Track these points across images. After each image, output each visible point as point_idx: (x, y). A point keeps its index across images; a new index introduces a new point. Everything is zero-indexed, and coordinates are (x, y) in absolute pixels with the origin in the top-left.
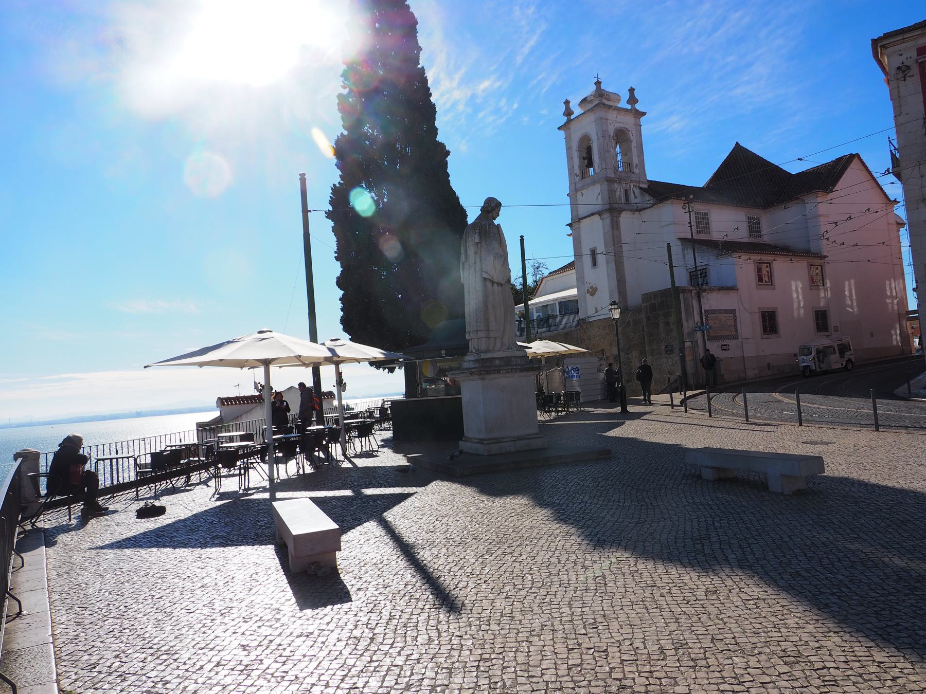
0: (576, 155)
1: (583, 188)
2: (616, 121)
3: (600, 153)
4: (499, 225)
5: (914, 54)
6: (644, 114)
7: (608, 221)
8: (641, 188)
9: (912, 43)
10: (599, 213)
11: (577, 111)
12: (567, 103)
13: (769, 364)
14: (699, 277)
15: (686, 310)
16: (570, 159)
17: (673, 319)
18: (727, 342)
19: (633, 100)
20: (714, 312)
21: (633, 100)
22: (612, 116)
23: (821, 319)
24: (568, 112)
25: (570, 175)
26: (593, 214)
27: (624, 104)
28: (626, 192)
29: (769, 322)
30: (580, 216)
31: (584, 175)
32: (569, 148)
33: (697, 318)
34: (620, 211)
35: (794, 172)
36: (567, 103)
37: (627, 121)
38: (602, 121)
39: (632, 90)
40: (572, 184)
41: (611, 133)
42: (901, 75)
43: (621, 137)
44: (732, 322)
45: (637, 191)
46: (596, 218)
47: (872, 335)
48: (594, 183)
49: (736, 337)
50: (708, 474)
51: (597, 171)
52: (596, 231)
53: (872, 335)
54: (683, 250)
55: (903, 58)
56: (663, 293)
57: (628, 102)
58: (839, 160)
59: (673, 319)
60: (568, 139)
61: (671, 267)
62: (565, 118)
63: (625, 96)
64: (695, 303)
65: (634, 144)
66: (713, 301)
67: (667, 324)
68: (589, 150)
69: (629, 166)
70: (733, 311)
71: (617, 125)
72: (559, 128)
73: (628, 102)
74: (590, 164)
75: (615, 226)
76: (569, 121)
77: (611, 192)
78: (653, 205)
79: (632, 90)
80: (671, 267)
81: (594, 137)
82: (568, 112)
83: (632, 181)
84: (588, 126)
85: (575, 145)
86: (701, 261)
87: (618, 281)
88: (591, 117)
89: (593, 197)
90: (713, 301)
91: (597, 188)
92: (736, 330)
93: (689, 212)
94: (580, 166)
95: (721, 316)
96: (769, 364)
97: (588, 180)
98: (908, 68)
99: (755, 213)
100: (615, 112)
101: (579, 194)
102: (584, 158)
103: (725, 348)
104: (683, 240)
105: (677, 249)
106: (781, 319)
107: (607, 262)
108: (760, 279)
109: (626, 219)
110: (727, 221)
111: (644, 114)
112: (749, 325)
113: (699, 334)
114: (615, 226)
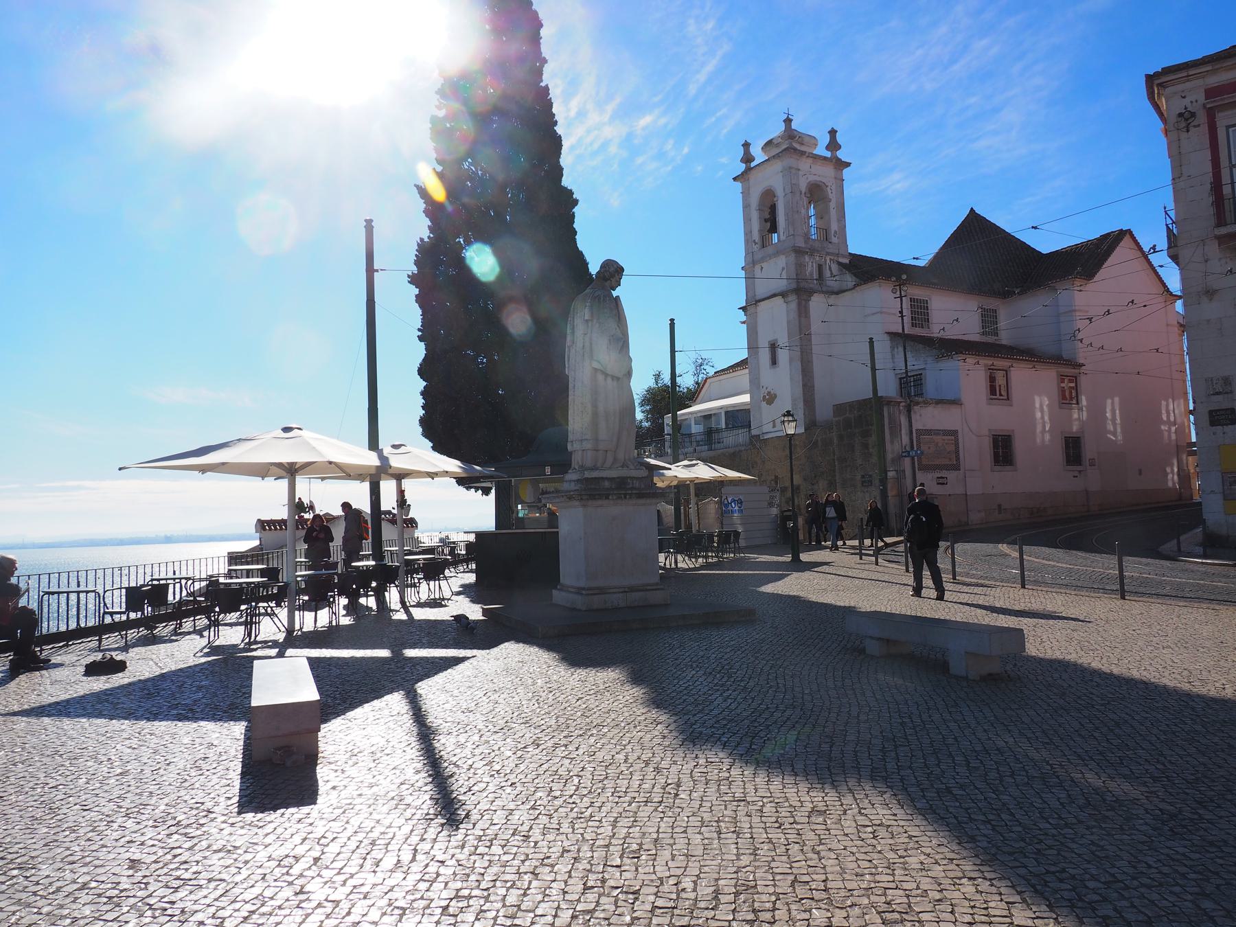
0: (755, 216)
1: (763, 260)
2: (810, 173)
3: (787, 215)
4: (618, 297)
5: (1201, 97)
6: (848, 165)
7: (794, 305)
8: (840, 264)
9: (1199, 82)
10: (783, 294)
11: (759, 156)
12: (746, 145)
13: (999, 506)
14: (911, 386)
15: (890, 428)
16: (747, 220)
17: (873, 439)
18: (944, 474)
19: (834, 145)
20: (929, 432)
21: (834, 145)
22: (804, 164)
23: (1073, 449)
24: (747, 158)
25: (747, 242)
26: (774, 296)
27: (821, 150)
28: (820, 267)
29: (1003, 449)
30: (758, 298)
31: (764, 242)
32: (746, 206)
33: (905, 439)
34: (811, 292)
35: (1045, 251)
36: (746, 145)
37: (824, 173)
38: (790, 172)
39: (833, 133)
40: (749, 252)
41: (803, 187)
42: (1183, 124)
43: (816, 193)
44: (953, 448)
45: (835, 267)
46: (779, 300)
47: (1140, 472)
48: (778, 253)
49: (956, 467)
50: (873, 648)
51: (782, 238)
52: (777, 315)
53: (1140, 472)
54: (892, 348)
55: (1187, 102)
56: (862, 404)
57: (827, 148)
58: (1105, 237)
59: (873, 439)
60: (746, 194)
61: (874, 369)
62: (743, 166)
64: (904, 421)
65: (832, 205)
66: (928, 418)
67: (866, 446)
68: (773, 208)
69: (825, 233)
70: (954, 433)
71: (812, 178)
72: (735, 179)
73: (827, 148)
74: (773, 228)
75: (803, 311)
76: (749, 169)
77: (800, 266)
78: (855, 286)
79: (833, 133)
80: (874, 369)
81: (780, 192)
82: (747, 158)
83: (828, 254)
84: (773, 177)
86: (915, 364)
87: (804, 386)
88: (778, 166)
89: (776, 272)
90: (928, 418)
91: (781, 261)
92: (958, 459)
93: (901, 297)
94: (760, 231)
95: (938, 438)
96: (999, 506)
97: (769, 250)
98: (1193, 115)
99: (991, 303)
100: (810, 161)
101: (757, 268)
102: (766, 221)
103: (942, 482)
104: (893, 335)
105: (883, 346)
106: (1019, 447)
107: (791, 360)
109: (817, 303)
110: (954, 314)
111: (848, 165)
112: (975, 450)
113: (907, 461)
114: (803, 311)
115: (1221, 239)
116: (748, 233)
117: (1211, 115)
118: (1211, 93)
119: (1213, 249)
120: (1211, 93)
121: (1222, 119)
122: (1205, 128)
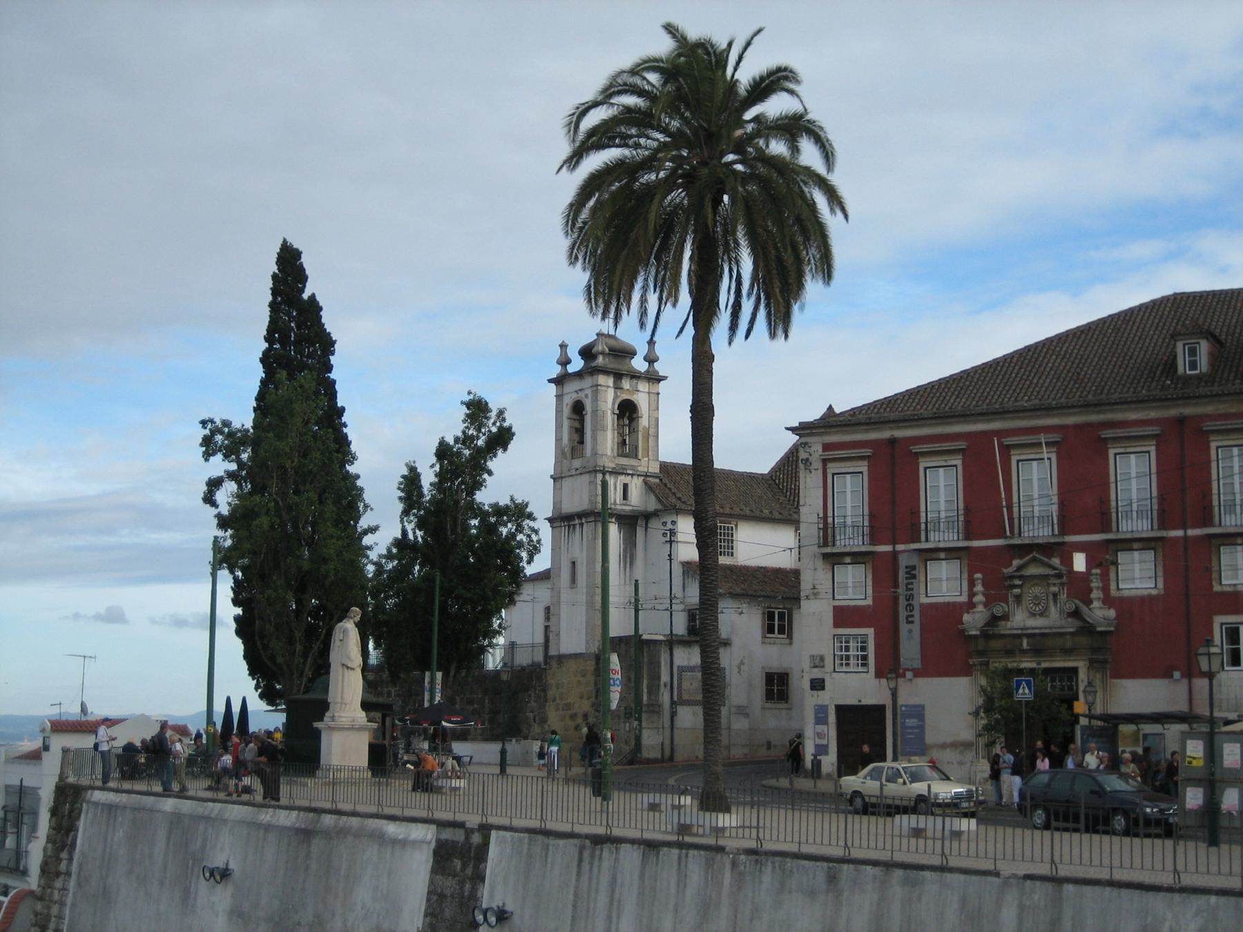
5: (820, 448)
6: (664, 378)
12: (563, 346)
21: (651, 359)
24: (565, 362)
32: (559, 411)
36: (563, 346)
40: (560, 455)
57: (645, 359)
60: (559, 397)
63: (642, 350)
72: (550, 381)
82: (565, 362)
85: (567, 411)
108: (770, 629)
111: (664, 378)
115: (826, 557)
116: (558, 440)
117: (825, 462)
118: (827, 447)
119: (820, 564)
120: (827, 447)
121: (830, 472)
122: (820, 472)
